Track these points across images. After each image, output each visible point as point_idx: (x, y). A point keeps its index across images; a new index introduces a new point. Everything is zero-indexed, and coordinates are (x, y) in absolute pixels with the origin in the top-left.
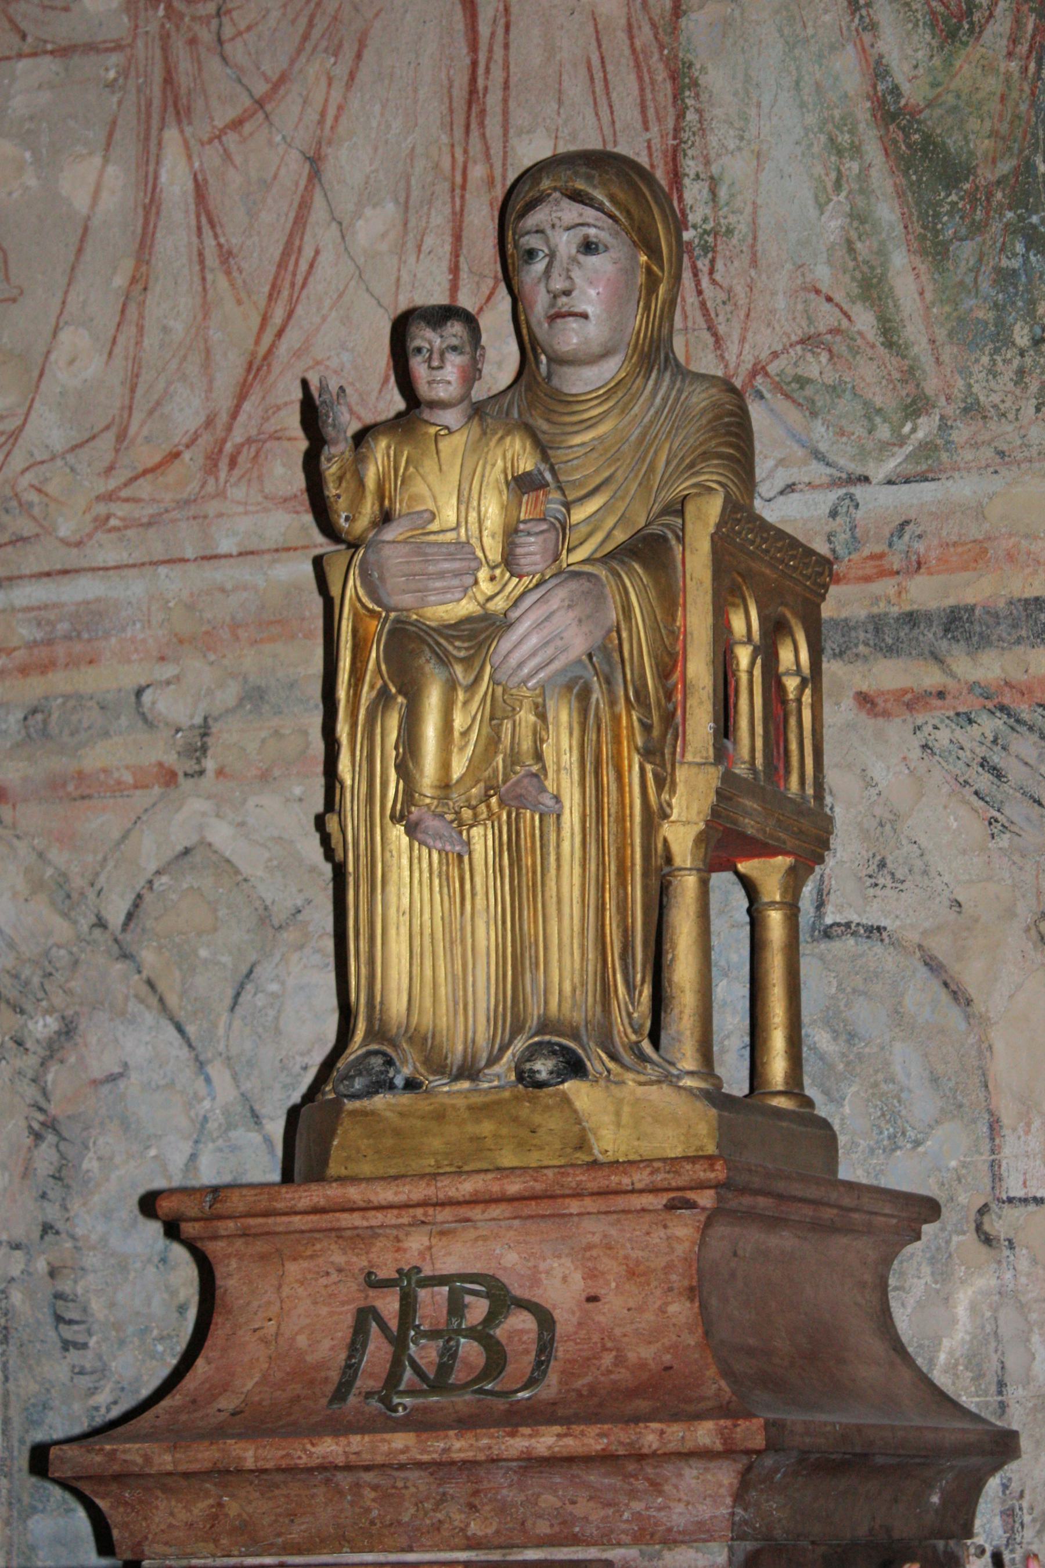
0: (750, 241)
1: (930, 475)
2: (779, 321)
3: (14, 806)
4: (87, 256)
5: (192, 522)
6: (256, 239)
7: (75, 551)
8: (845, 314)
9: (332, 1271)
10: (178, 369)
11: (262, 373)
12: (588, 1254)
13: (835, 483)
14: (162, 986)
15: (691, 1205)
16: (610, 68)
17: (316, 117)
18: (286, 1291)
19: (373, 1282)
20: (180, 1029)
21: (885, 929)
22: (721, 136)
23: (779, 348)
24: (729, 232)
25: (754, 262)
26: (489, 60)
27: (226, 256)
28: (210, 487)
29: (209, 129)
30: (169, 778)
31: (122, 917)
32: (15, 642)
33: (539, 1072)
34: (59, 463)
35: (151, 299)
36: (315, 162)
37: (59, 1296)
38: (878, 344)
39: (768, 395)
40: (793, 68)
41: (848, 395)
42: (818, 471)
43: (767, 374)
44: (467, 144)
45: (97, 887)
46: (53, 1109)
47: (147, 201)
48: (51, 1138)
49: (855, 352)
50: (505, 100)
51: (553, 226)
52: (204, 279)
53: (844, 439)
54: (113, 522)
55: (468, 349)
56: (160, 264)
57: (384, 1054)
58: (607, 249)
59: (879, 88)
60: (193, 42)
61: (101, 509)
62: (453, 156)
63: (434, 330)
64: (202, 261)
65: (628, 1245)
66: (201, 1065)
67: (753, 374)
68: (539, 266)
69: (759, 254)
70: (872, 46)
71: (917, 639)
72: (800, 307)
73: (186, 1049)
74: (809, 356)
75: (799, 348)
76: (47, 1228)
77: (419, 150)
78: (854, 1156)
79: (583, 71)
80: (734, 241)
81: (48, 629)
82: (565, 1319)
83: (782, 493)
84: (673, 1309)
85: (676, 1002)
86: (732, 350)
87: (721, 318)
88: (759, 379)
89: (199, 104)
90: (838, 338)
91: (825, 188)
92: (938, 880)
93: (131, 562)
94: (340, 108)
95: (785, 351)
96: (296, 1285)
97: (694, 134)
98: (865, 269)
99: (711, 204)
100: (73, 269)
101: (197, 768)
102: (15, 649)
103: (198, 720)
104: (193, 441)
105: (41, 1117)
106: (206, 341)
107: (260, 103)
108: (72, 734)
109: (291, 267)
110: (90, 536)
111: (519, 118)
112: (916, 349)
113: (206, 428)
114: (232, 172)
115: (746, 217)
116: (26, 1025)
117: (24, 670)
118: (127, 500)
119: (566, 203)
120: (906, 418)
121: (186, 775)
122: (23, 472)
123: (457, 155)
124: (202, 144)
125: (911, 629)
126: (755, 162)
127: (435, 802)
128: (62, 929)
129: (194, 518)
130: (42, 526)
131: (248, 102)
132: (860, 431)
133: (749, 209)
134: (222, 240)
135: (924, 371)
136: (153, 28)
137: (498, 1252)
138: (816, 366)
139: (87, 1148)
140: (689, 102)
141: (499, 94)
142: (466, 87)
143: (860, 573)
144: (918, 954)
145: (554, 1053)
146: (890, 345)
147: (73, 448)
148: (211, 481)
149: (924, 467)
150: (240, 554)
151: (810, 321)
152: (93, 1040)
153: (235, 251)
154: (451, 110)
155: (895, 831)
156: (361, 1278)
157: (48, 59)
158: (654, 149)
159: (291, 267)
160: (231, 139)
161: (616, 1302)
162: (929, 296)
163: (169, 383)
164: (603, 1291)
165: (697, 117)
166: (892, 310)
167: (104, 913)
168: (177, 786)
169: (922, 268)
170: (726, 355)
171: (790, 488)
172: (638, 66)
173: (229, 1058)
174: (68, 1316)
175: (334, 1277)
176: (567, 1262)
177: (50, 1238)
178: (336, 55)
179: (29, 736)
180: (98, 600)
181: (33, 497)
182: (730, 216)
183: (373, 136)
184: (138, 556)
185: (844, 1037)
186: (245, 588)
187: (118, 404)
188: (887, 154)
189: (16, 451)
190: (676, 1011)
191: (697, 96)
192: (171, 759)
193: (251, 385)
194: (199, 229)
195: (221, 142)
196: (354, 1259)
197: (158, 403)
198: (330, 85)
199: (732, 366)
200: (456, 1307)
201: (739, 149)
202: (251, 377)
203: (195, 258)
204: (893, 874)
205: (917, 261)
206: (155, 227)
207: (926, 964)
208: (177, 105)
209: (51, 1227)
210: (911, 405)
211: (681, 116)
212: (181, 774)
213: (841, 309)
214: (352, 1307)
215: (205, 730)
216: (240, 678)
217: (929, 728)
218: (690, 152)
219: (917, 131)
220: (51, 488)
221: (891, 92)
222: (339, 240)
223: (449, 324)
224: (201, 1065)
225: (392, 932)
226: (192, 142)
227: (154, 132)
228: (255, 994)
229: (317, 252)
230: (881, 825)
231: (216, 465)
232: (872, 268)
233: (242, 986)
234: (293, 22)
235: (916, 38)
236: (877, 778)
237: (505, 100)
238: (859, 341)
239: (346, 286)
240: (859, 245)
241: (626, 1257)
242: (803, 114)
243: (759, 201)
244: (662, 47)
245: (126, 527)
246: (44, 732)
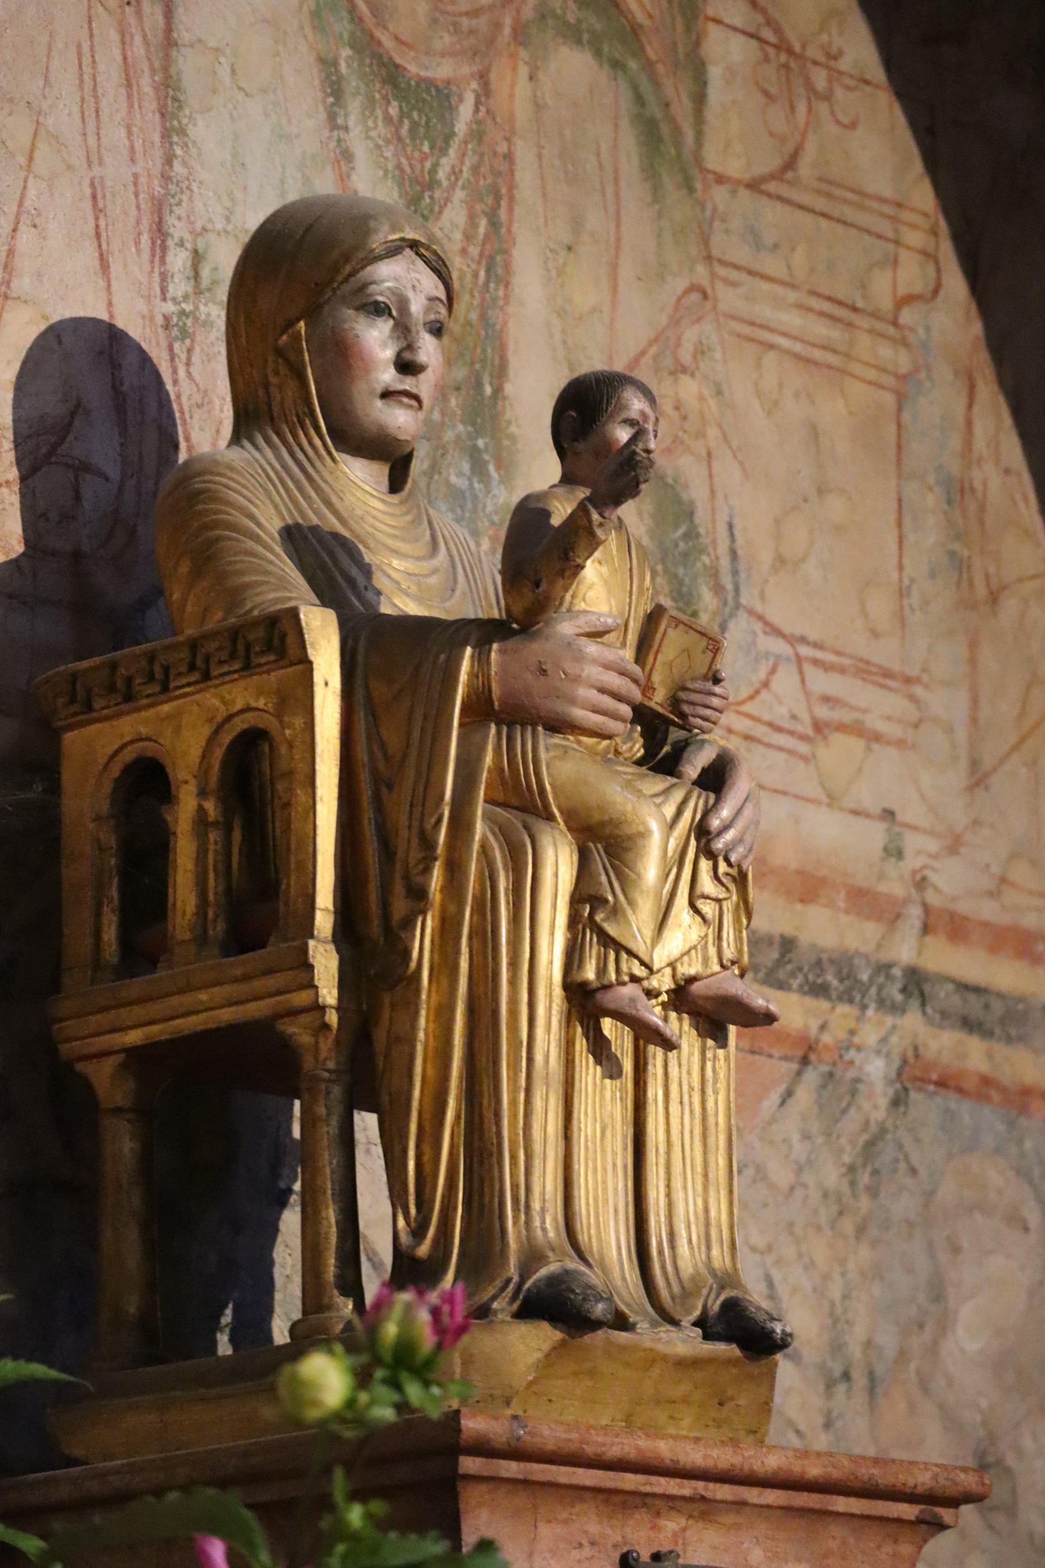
70: (349, 177)
97: (182, 192)
99: (192, 282)
137: (746, 1545)
175: (587, 1551)
196: (609, 1531)
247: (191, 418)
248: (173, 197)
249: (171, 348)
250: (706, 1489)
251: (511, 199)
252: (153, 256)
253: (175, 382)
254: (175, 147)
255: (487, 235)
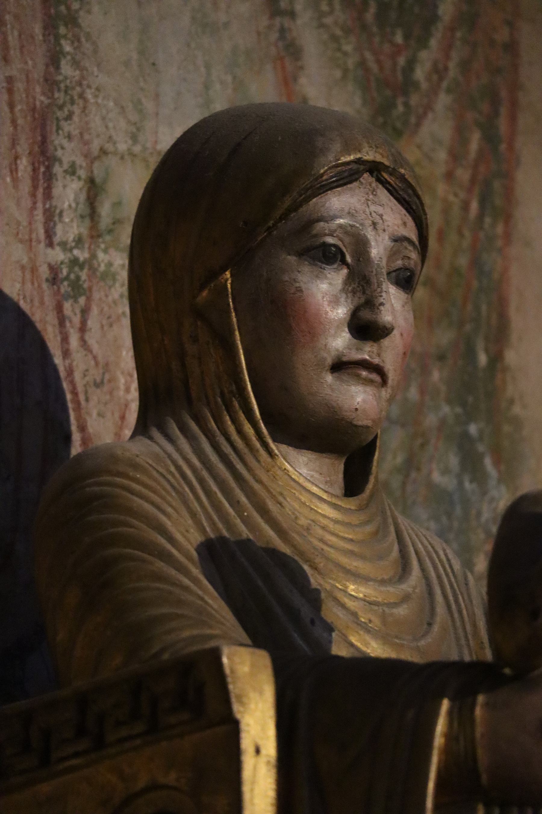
70: (295, 79)
97: (73, 102)
99: (87, 221)
247: (87, 400)
249: (59, 308)
251: (514, 104)
252: (35, 187)
253: (66, 354)
254: (63, 42)
255: (480, 152)
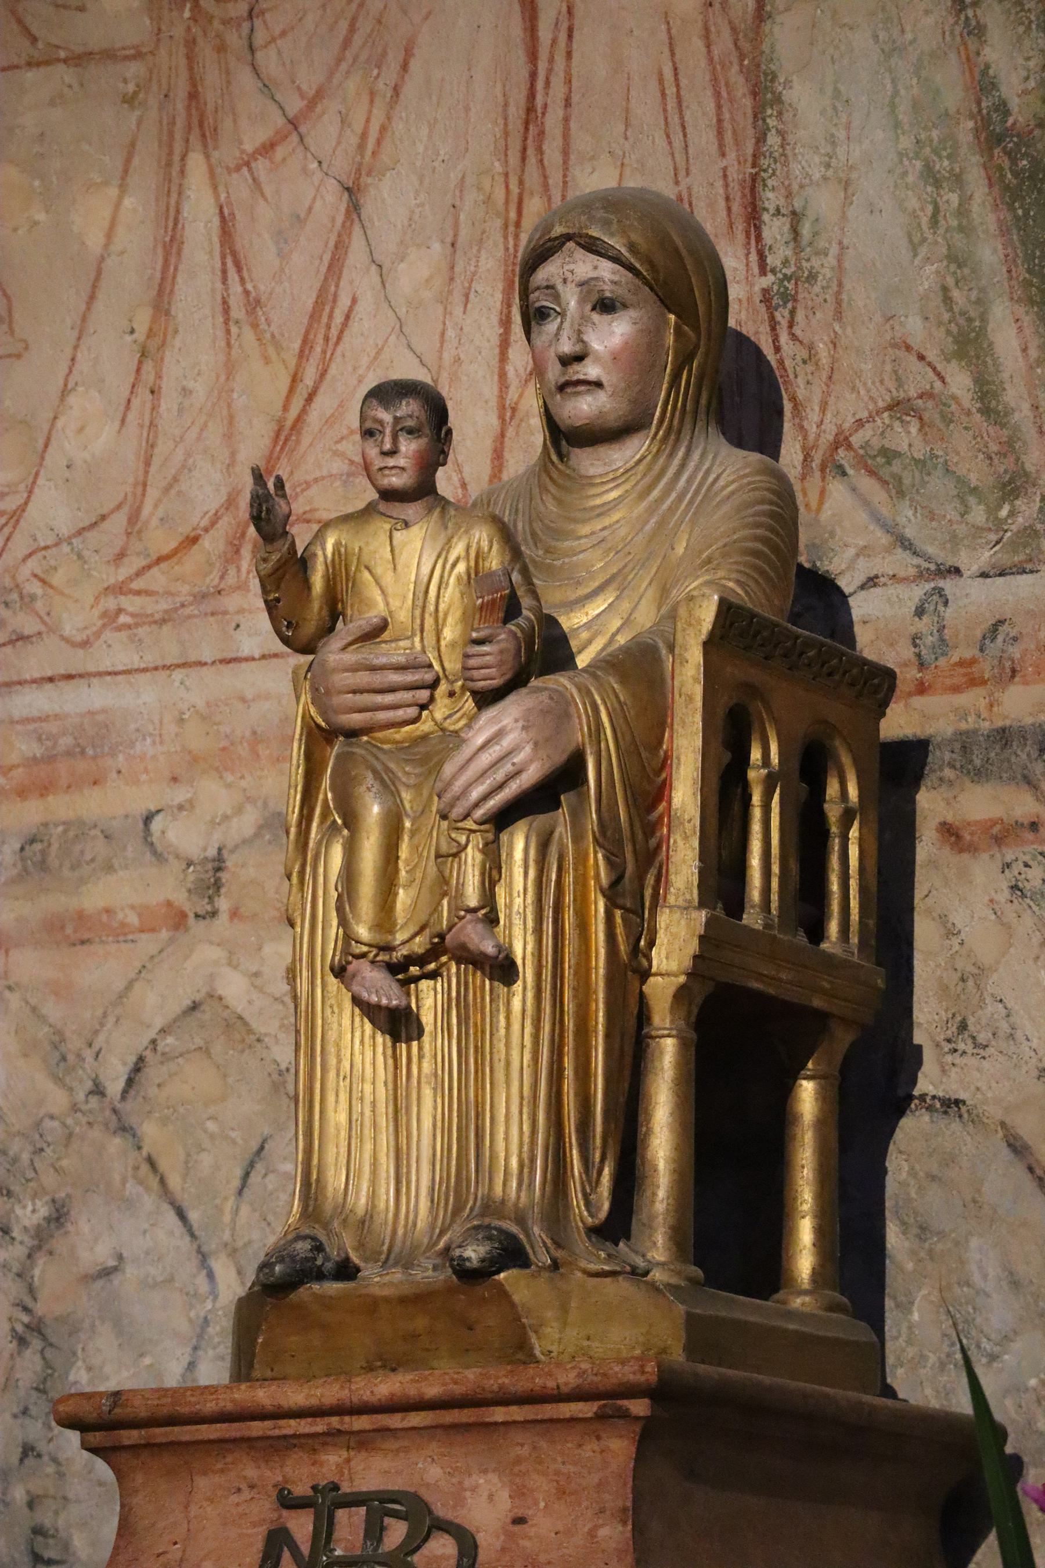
0: (835, 289)
1: (1029, 567)
2: (865, 384)
3: (7, 952)
4: (99, 305)
5: (211, 619)
6: (287, 284)
7: (80, 652)
8: (938, 374)
9: (244, 1486)
10: (199, 439)
11: (291, 444)
12: (516, 1469)
13: (922, 575)
14: (163, 1164)
15: (625, 1415)
16: (684, 82)
17: (354, 141)
18: (194, 1510)
19: (288, 1502)
20: (181, 1215)
21: (964, 1102)
22: (805, 163)
23: (864, 415)
24: (812, 277)
25: (838, 315)
26: (550, 71)
27: (254, 304)
28: (231, 579)
29: (238, 154)
30: (178, 920)
31: (121, 1084)
32: (14, 758)
33: (469, 1259)
34: (65, 548)
35: (169, 356)
36: (352, 192)
37: (38, 1531)
38: (974, 410)
39: (850, 472)
40: (888, 82)
41: (939, 472)
42: (902, 562)
43: (850, 447)
44: (523, 171)
45: (96, 1047)
46: (40, 1309)
47: (168, 239)
48: (36, 1343)
49: (948, 420)
50: (566, 120)
51: (565, 281)
52: (228, 332)
53: (934, 524)
54: (123, 619)
55: (427, 431)
56: (180, 315)
57: (314, 1239)
58: (625, 306)
59: (984, 105)
60: (221, 48)
61: (110, 603)
62: (507, 187)
63: (386, 409)
64: (226, 310)
65: (559, 1459)
66: (203, 1257)
67: (836, 445)
68: (551, 326)
69: (844, 305)
70: (978, 54)
71: (1009, 761)
72: (888, 367)
73: (188, 1239)
74: (897, 424)
75: (886, 415)
76: (28, 1450)
77: (470, 180)
78: (922, 1371)
79: (653, 86)
80: (817, 289)
81: (49, 743)
82: (488, 1542)
83: (862, 587)
84: (603, 1532)
85: (648, 1182)
86: (813, 416)
87: (801, 381)
88: (841, 452)
89: (227, 124)
90: (930, 404)
91: (919, 225)
92: (1025, 1047)
93: (143, 666)
94: (383, 129)
95: (871, 419)
96: (205, 1504)
97: (775, 162)
98: (962, 321)
99: (792, 245)
100: (84, 319)
101: (209, 908)
102: (11, 768)
103: (212, 852)
104: (213, 523)
105: (26, 1319)
106: (229, 406)
107: (294, 123)
108: (73, 868)
109: (325, 319)
110: (98, 634)
111: (581, 142)
112: (1017, 416)
113: (227, 509)
114: (261, 201)
115: (831, 260)
116: (12, 1210)
117: (22, 793)
118: (138, 593)
119: (580, 253)
120: (1003, 500)
121: (197, 916)
122: (25, 560)
123: (511, 187)
124: (229, 171)
125: (1002, 749)
126: (842, 195)
127: (374, 951)
128: (57, 1100)
129: (213, 614)
130: (44, 623)
131: (281, 121)
132: (952, 515)
133: (834, 250)
134: (249, 287)
135: (1025, 443)
136: (179, 31)
137: (420, 1465)
138: (906, 437)
139: (74, 1354)
140: (772, 122)
141: (561, 113)
142: (523, 102)
143: (948, 682)
144: (1000, 1134)
145: (490, 1238)
146: (986, 411)
147: (80, 532)
148: (232, 571)
149: (1022, 557)
150: (264, 657)
151: (900, 383)
152: (85, 1228)
153: (263, 299)
154: (506, 134)
155: (978, 986)
156: (274, 1494)
157: (62, 67)
158: (730, 179)
159: (325, 319)
160: (261, 166)
161: (543, 1525)
162: (1034, 353)
163: (188, 455)
164: (530, 1512)
165: (779, 140)
166: (992, 369)
167: (102, 1078)
168: (187, 930)
169: (1027, 320)
170: (805, 423)
171: (871, 582)
172: (715, 80)
173: (235, 1250)
174: (47, 1554)
175: (246, 1494)
176: (494, 1478)
177: (30, 1461)
178: (379, 66)
179: (25, 869)
180: (104, 711)
181: (35, 588)
182: (813, 259)
183: (418, 164)
184: (150, 659)
185: (915, 1230)
186: (267, 697)
187: (131, 480)
188: (991, 185)
189: (17, 537)
190: (648, 1193)
191: (780, 113)
192: (181, 898)
193: (279, 458)
194: (224, 272)
195: (250, 169)
196: (268, 1473)
197: (175, 479)
198: (372, 101)
199: (812, 437)
200: (374, 1531)
201: (825, 178)
202: (278, 448)
203: (219, 308)
204: (974, 1038)
205: (1021, 310)
206: (176, 269)
207: (1009, 1145)
208: (201, 125)
209: (33, 1449)
210: (1010, 483)
211: (761, 139)
212: (191, 915)
213: (934, 369)
214: (262, 1531)
215: (218, 864)
216: (260, 803)
217: (1018, 867)
218: (770, 183)
219: (1026, 155)
220: (57, 579)
221: (996, 110)
222: (379, 286)
223: (404, 403)
224: (203, 1257)
225: (331, 1098)
226: (218, 170)
227: (176, 158)
228: (266, 1175)
229: (354, 301)
230: (963, 980)
231: (237, 552)
232: (970, 320)
233: (252, 1165)
234: (331, 29)
235: (1027, 43)
236: (959, 925)
237: (566, 120)
238: (954, 407)
239: (386, 341)
240: (955, 294)
241: (557, 1473)
242: (898, 138)
243: (845, 242)
244: (742, 57)
245: (137, 625)
246: (43, 865)
248: (765, 171)
249: (772, 318)
250: (342, 1423)
252: (748, 237)
253: (777, 349)
254: (768, 120)
